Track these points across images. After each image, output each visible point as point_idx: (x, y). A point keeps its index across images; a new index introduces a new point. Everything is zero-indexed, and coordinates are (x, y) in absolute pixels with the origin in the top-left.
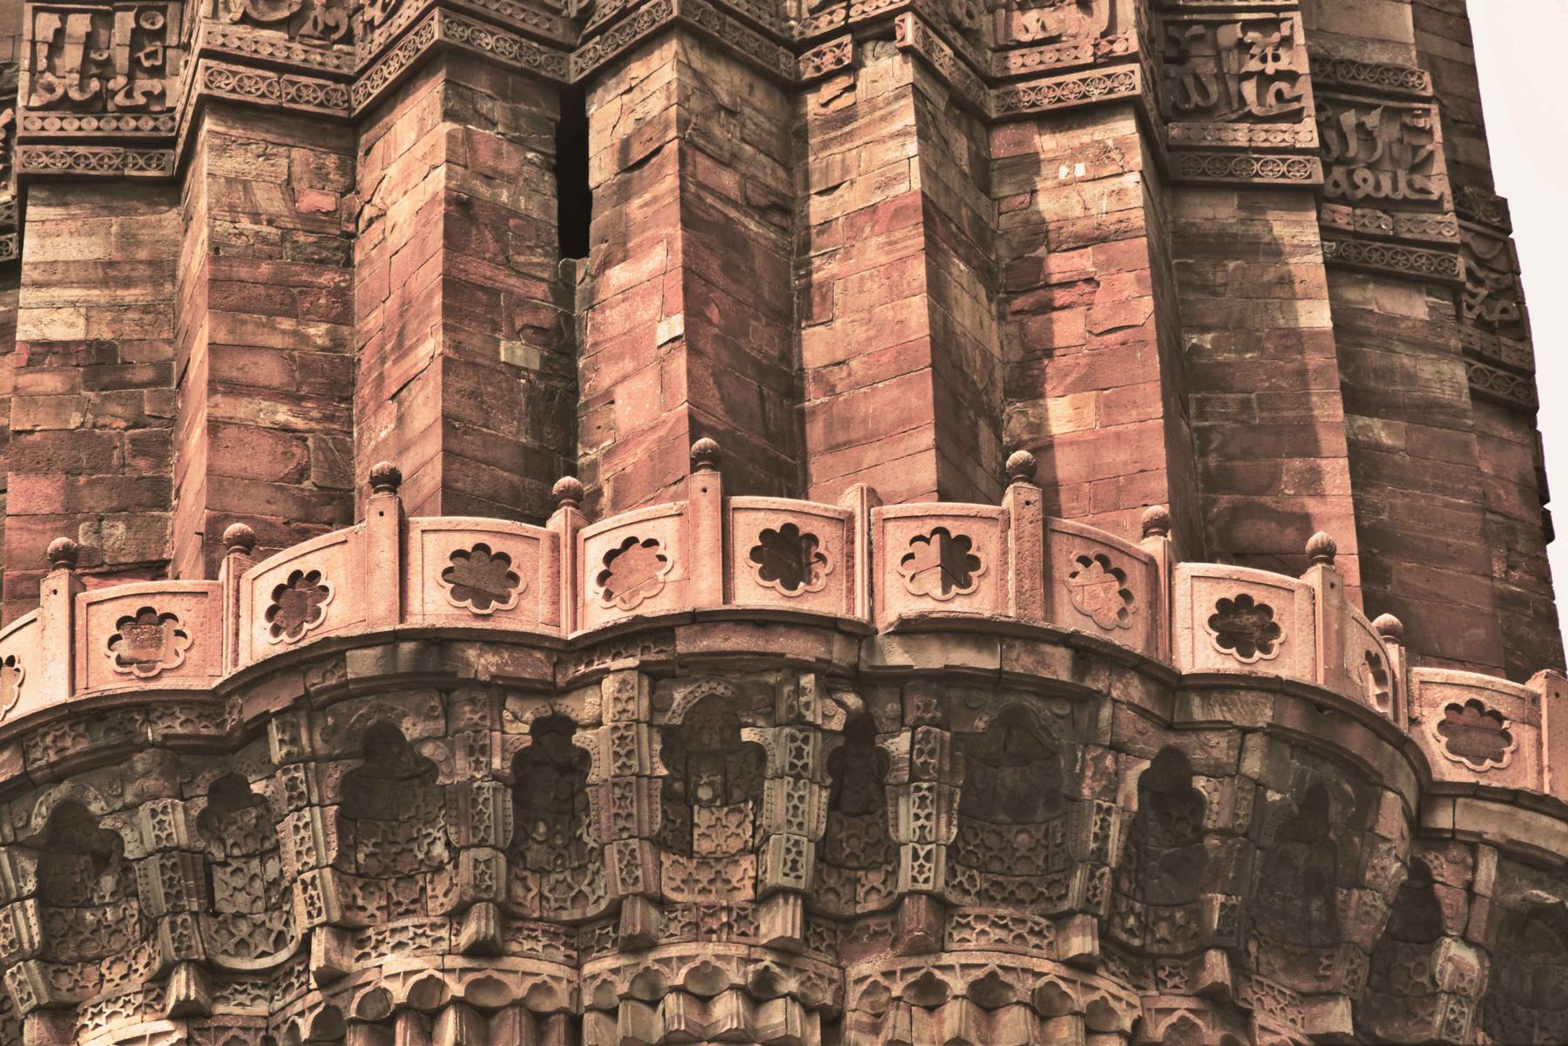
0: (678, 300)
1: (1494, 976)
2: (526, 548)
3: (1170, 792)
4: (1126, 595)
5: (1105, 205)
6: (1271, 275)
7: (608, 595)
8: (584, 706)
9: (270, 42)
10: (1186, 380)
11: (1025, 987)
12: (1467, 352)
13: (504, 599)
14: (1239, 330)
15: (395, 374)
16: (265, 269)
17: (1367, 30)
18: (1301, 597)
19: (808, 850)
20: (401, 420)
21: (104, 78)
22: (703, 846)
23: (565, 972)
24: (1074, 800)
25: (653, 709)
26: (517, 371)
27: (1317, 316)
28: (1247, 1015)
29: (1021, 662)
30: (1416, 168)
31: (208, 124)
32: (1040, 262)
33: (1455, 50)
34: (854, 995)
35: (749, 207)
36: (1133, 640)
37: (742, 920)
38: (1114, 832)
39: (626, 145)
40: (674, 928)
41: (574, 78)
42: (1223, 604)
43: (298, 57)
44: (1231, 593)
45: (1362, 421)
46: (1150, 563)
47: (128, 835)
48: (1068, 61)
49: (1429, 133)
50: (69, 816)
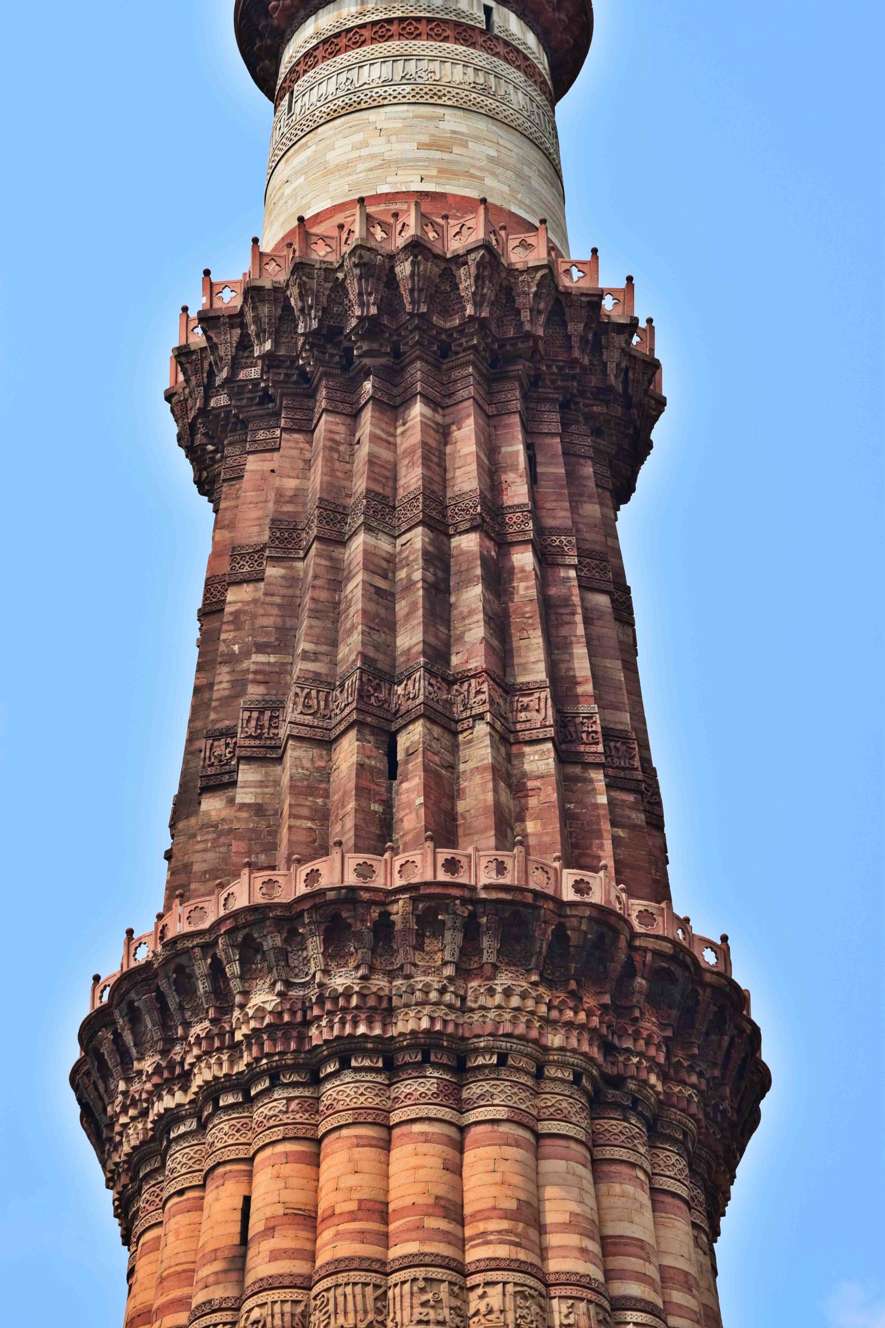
0: (422, 793)
1: (650, 988)
2: (378, 863)
3: (560, 935)
4: (548, 878)
5: (543, 767)
6: (590, 788)
7: (401, 877)
8: (394, 908)
9: (308, 719)
10: (567, 818)
11: (518, 990)
12: (645, 811)
13: (371, 878)
14: (580, 803)
15: (341, 813)
16: (305, 783)
17: (617, 719)
18: (598, 879)
19: (457, 950)
20: (343, 826)
21: (262, 729)
22: (427, 949)
23: (387, 984)
24: (532, 936)
25: (413, 909)
26: (376, 812)
27: (603, 799)
28: (581, 998)
29: (519, 897)
30: (630, 759)
31: (290, 742)
32: (525, 783)
33: (641, 726)
34: (470, 992)
35: (443, 767)
36: (550, 891)
37: (439, 970)
38: (544, 946)
39: (408, 749)
40: (419, 972)
41: (393, 730)
42: (576, 881)
43: (315, 724)
44: (578, 878)
45: (615, 829)
46: (556, 869)
47: (264, 943)
48: (533, 727)
49: (634, 749)
50: (248, 938)
